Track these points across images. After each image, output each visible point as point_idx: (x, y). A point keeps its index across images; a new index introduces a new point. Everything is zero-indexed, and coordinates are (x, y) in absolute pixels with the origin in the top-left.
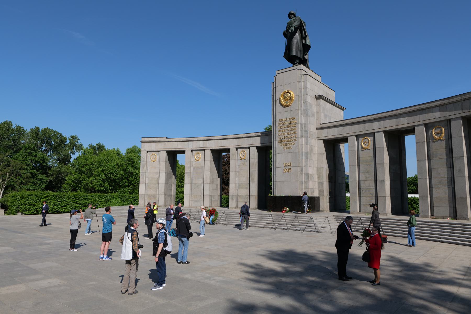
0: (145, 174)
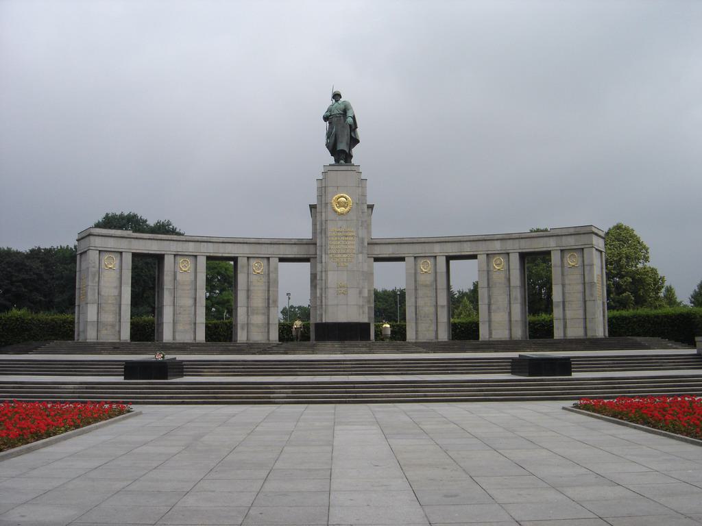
0: (96, 288)
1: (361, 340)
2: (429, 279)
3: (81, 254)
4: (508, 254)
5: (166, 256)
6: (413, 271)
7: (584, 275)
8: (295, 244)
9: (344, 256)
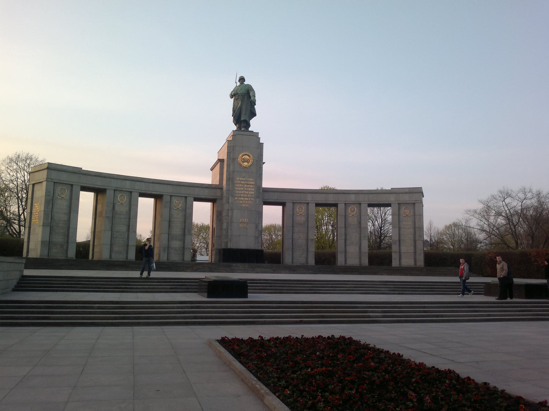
0: (50, 213)
1: (257, 262)
2: (303, 219)
3: (34, 185)
4: (360, 204)
5: (108, 191)
6: (291, 213)
7: (415, 222)
8: (206, 188)
9: (246, 199)
